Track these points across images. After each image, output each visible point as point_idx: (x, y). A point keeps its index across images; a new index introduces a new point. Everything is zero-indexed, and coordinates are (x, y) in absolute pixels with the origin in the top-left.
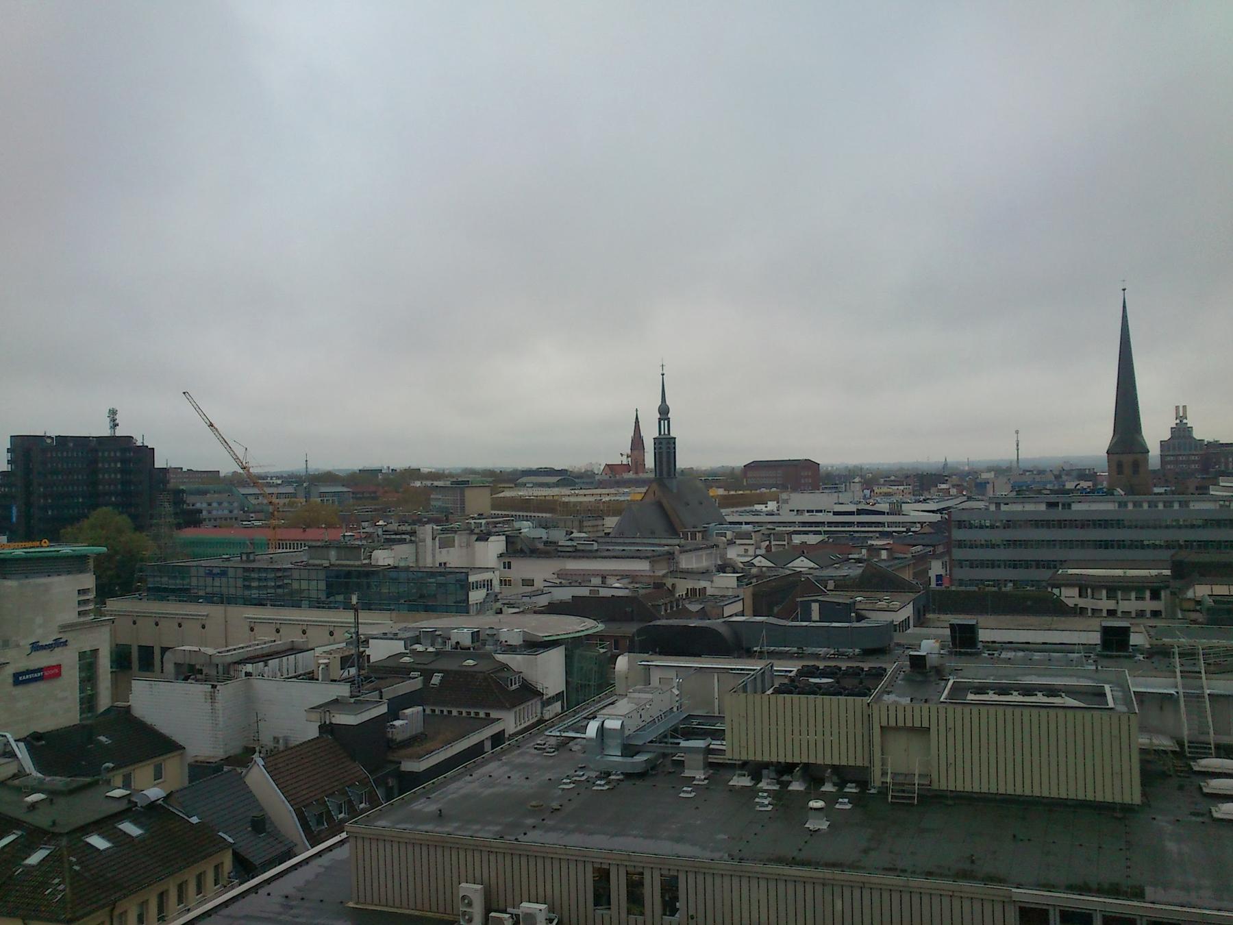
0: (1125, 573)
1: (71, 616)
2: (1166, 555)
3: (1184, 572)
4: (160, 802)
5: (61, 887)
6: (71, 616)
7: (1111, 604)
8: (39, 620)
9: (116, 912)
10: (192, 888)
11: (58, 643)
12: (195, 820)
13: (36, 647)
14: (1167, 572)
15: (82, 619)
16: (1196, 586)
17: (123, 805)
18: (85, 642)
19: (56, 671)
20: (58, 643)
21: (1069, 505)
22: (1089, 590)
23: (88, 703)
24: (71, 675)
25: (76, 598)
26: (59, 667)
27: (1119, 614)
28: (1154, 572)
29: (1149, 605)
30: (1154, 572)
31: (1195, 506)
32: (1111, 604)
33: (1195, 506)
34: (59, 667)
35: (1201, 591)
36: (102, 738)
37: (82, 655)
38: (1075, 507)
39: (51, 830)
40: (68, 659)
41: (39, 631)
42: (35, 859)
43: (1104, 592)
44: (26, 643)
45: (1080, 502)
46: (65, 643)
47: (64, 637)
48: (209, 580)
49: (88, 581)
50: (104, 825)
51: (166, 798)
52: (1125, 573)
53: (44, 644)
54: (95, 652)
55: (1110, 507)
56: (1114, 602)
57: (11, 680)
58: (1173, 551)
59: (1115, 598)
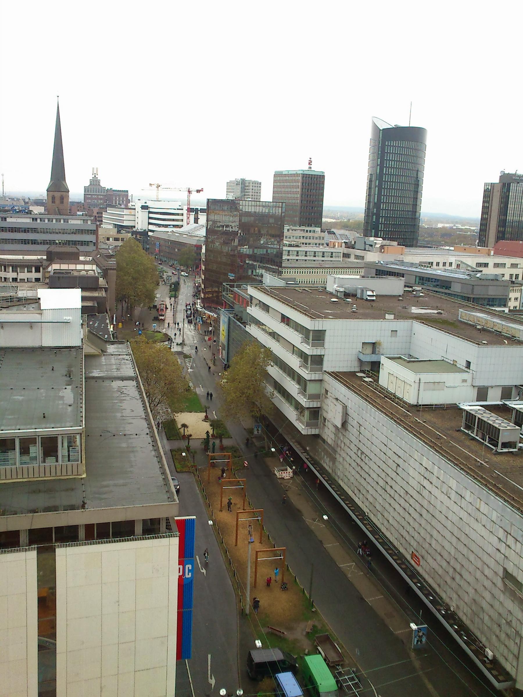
0: (23, 258)
2: (45, 247)
3: (52, 257)
7: (14, 275)
14: (45, 257)
16: (53, 265)
21: (5, 219)
22: (3, 267)
27: (19, 280)
28: (39, 257)
29: (34, 275)
30: (39, 257)
31: (71, 222)
32: (14, 275)
33: (71, 222)
35: (55, 266)
38: (8, 220)
43: (11, 268)
45: (11, 217)
52: (23, 258)
55: (28, 220)
56: (16, 274)
58: (47, 246)
59: (16, 271)
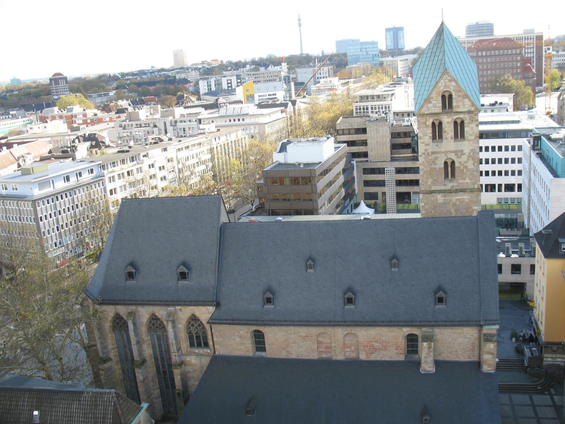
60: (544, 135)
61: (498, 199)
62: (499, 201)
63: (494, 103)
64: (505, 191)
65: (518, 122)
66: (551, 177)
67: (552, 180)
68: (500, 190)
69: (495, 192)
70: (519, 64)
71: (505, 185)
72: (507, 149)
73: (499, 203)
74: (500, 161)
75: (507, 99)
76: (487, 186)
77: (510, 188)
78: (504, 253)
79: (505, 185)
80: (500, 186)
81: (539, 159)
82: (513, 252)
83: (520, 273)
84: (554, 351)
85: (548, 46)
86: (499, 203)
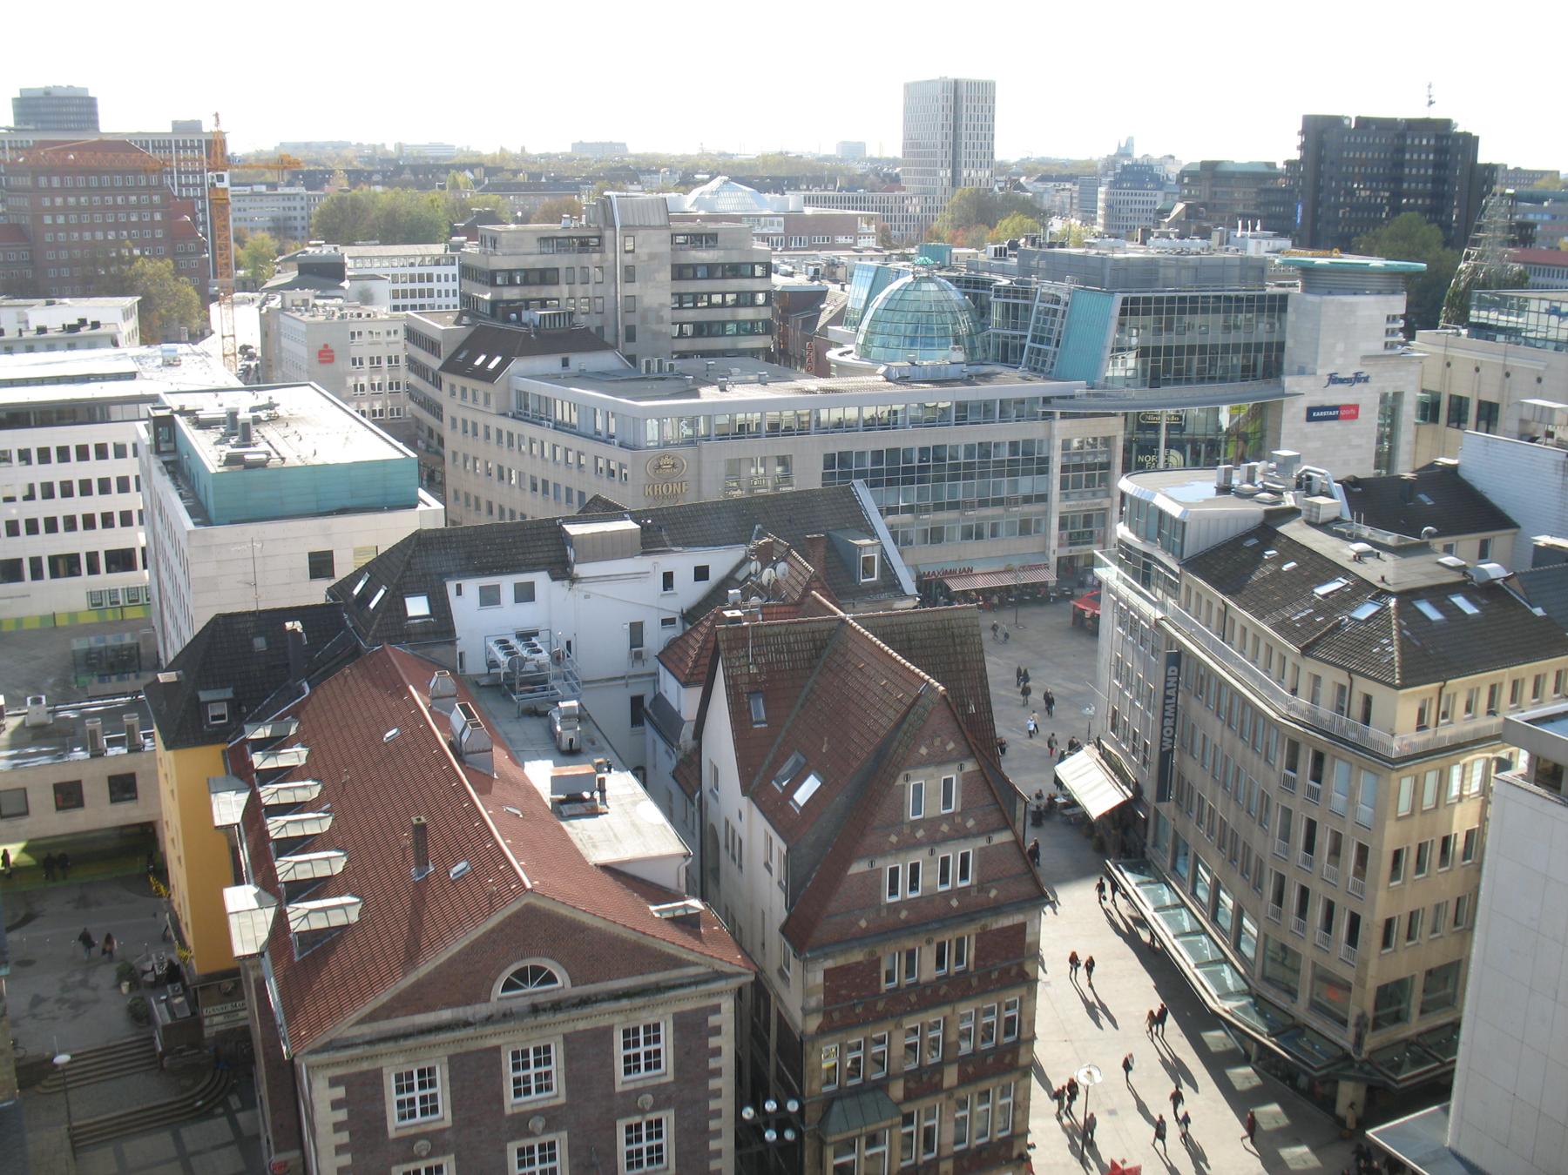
1: (1376, 347)
4: (1499, 582)
5: (1390, 649)
6: (1376, 347)
8: (1340, 347)
9: (1445, 692)
10: (1528, 689)
11: (1358, 378)
12: (1538, 611)
13: (1334, 379)
15: (1388, 352)
17: (1454, 577)
18: (1385, 380)
19: (1353, 411)
20: (1358, 378)
23: (1385, 459)
24: (1370, 419)
25: (1385, 326)
26: (1356, 407)
34: (1356, 407)
36: (1423, 497)
37: (1384, 398)
39: (1381, 585)
40: (1367, 398)
41: (1339, 361)
42: (1365, 611)
44: (1323, 372)
46: (1366, 380)
47: (1366, 372)
48: (1554, 319)
49: (1398, 304)
50: (1436, 595)
51: (1506, 579)
53: (1343, 376)
54: (1398, 396)
57: (1304, 415)
60: (182, 412)
61: (91, 594)
62: (96, 600)
63: (76, 322)
64: (109, 571)
65: (132, 376)
66: (188, 524)
67: (189, 532)
68: (93, 569)
69: (80, 575)
70: (158, 217)
71: (107, 553)
72: (83, 453)
73: (93, 605)
74: (86, 488)
75: (114, 312)
76: (53, 560)
77: (122, 560)
78: (84, 749)
79: (107, 553)
80: (92, 557)
81: (167, 477)
82: (111, 743)
83: (136, 798)
84: (228, 994)
85: (217, 170)
86: (93, 605)
